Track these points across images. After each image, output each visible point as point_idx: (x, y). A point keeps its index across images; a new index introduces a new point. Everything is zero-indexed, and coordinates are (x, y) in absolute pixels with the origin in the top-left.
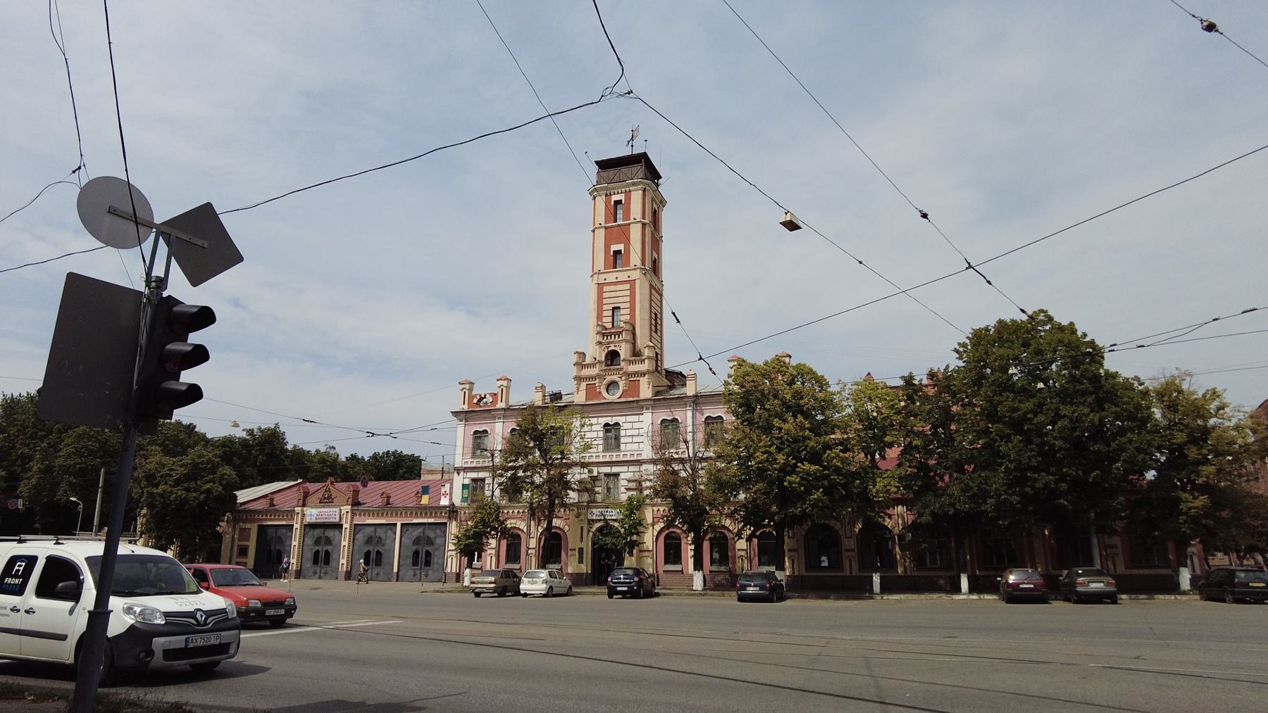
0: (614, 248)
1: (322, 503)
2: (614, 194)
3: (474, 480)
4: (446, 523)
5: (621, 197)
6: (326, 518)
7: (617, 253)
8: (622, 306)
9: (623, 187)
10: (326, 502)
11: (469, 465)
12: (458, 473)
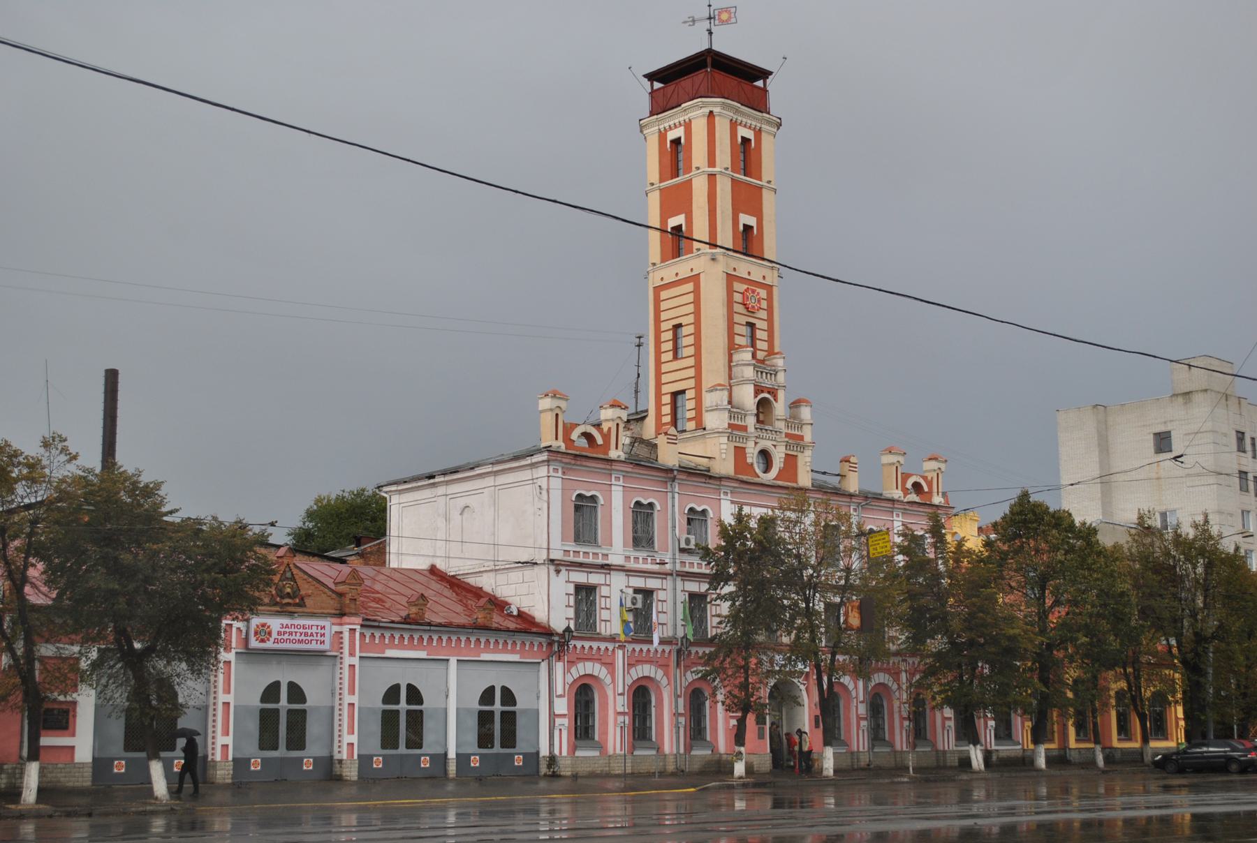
0: (746, 219)
1: (276, 604)
2: (740, 124)
3: (579, 588)
4: (539, 663)
5: (750, 134)
6: (300, 642)
7: (748, 228)
8: (759, 324)
9: (755, 118)
10: (288, 604)
11: (571, 558)
12: (558, 572)
